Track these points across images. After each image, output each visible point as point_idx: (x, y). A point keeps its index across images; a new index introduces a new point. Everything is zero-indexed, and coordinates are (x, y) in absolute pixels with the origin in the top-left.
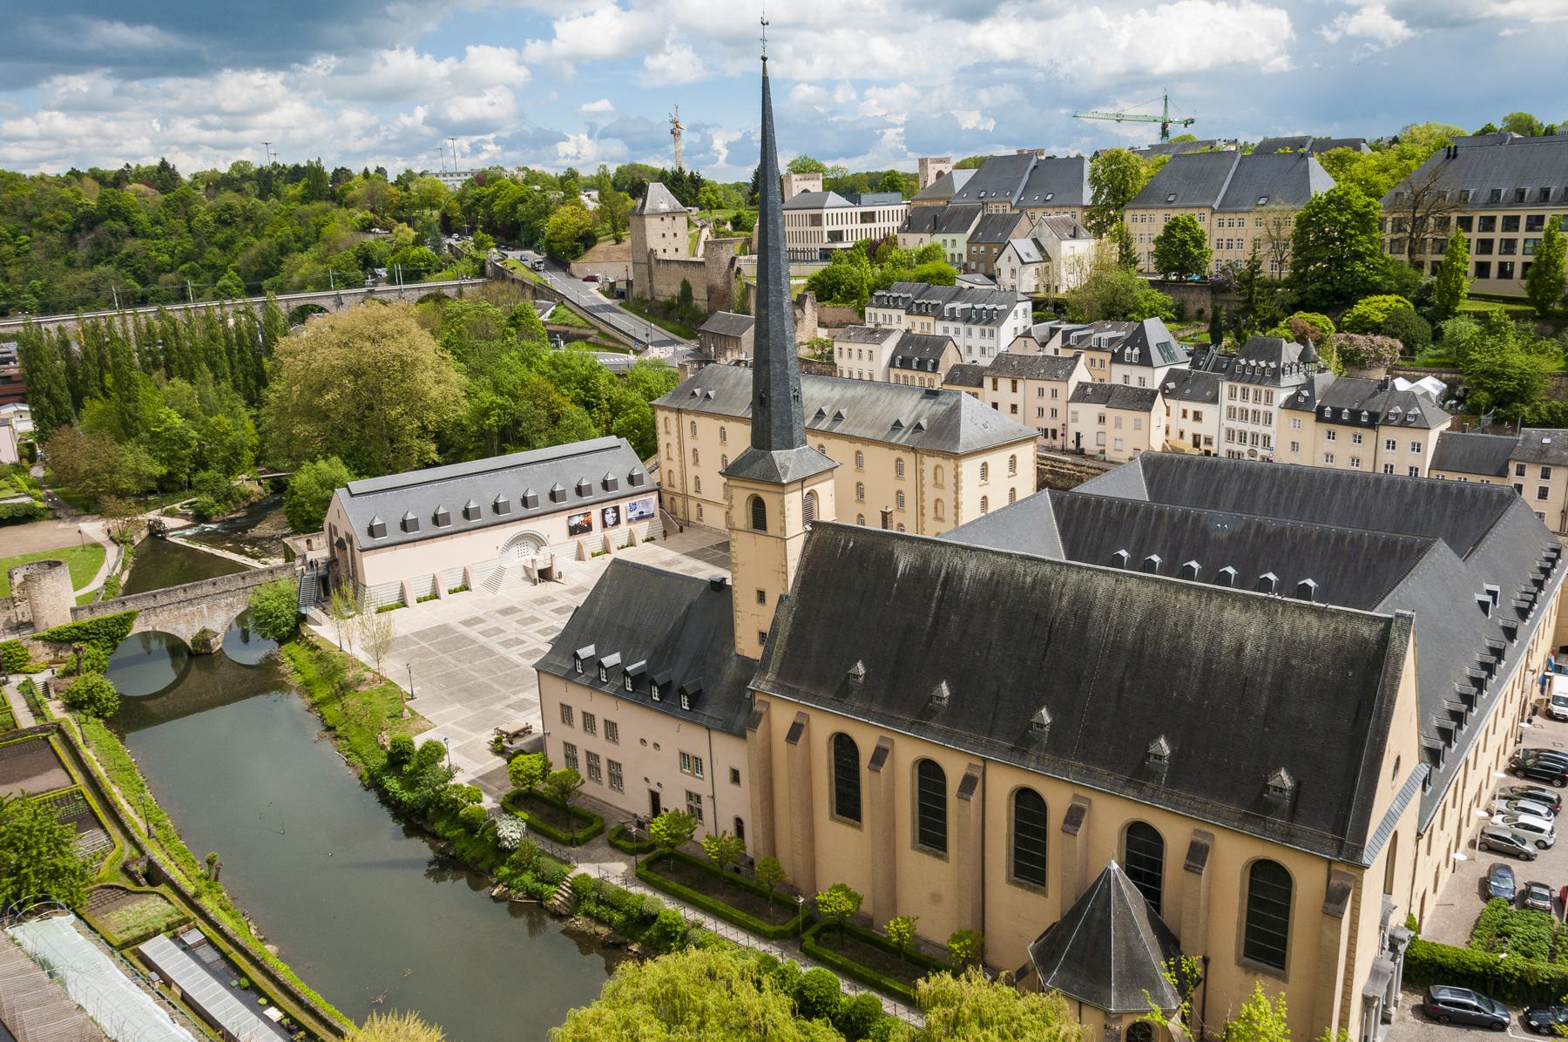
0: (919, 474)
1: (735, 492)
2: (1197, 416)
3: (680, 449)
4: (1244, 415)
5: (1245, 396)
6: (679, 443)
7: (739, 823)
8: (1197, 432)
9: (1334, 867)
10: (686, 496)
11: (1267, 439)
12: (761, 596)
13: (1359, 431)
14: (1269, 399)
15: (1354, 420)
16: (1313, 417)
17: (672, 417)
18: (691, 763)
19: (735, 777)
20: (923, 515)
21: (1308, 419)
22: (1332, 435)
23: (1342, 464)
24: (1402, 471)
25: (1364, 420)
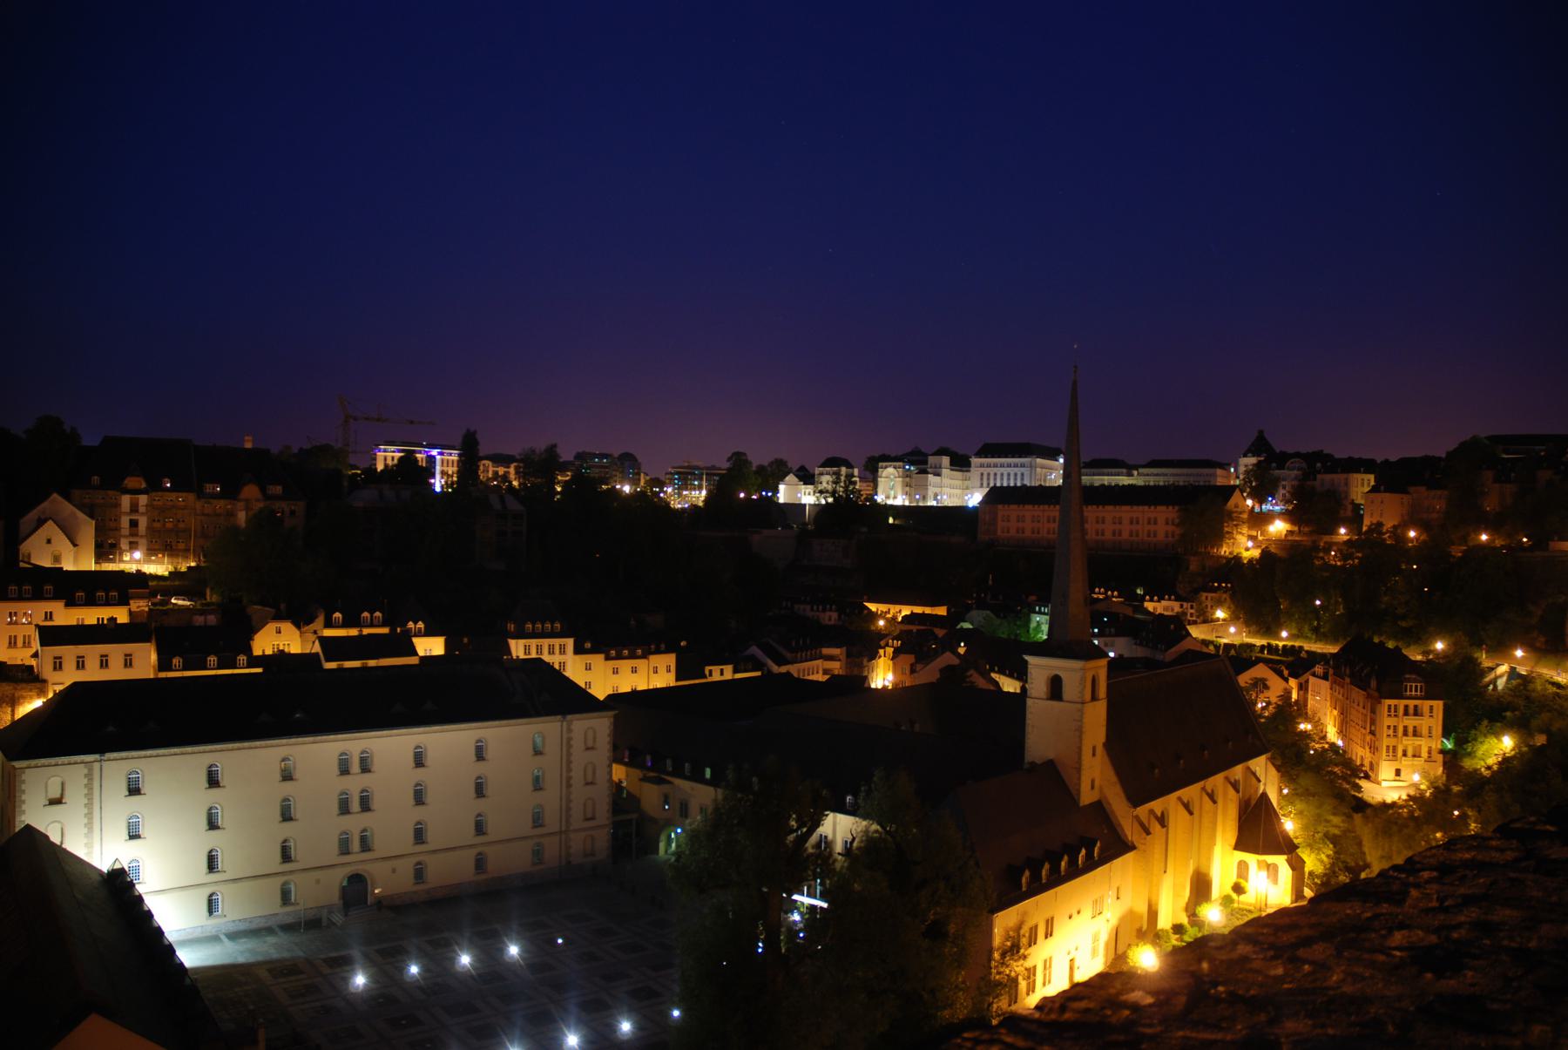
14: (563, 651)
15: (633, 656)
22: (616, 671)
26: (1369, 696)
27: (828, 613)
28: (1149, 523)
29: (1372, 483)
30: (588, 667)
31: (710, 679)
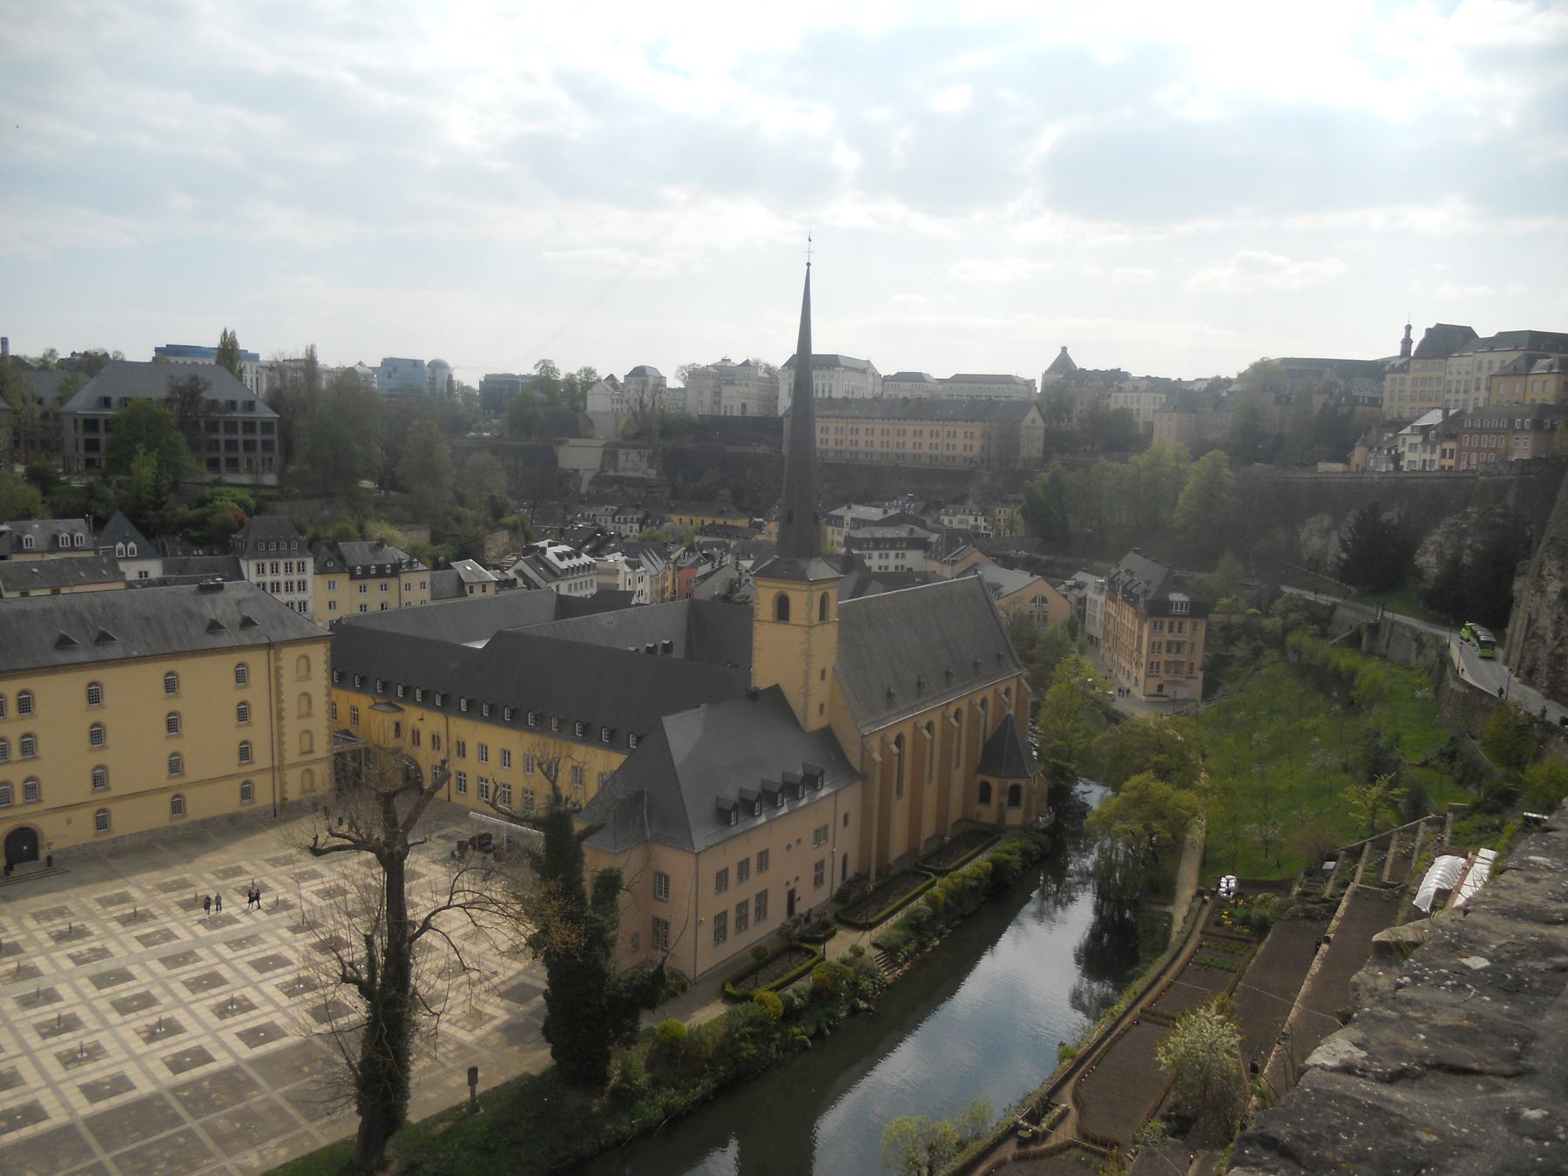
0: (275, 677)
5: (275, 570)
7: (845, 857)
13: (385, 580)
14: (302, 568)
15: (381, 572)
16: (347, 576)
20: (280, 718)
21: (342, 580)
22: (363, 589)
24: (415, 603)
25: (389, 571)
26: (1137, 614)
28: (949, 436)
29: (1164, 401)
30: (331, 585)
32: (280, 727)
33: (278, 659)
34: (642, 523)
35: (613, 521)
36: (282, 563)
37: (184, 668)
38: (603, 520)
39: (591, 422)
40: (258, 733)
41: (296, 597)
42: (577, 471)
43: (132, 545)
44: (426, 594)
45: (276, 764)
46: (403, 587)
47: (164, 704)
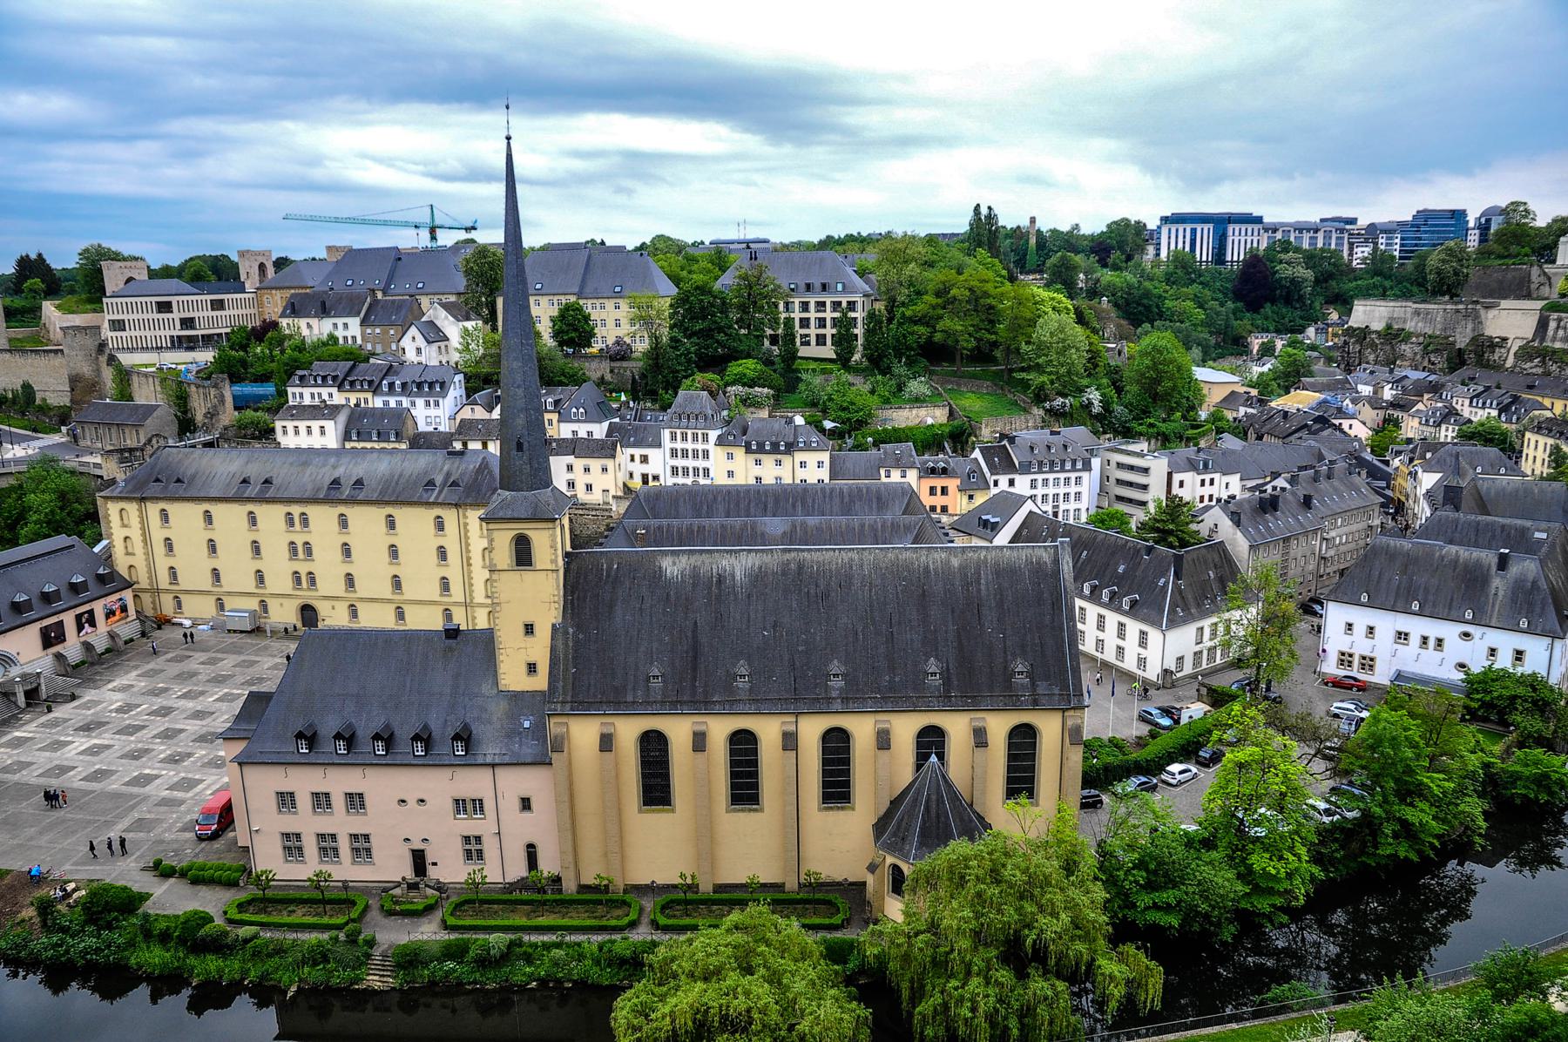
1: (496, 534)
2: (645, 459)
3: (145, 541)
4: (685, 453)
5: (684, 438)
6: (144, 534)
8: (645, 472)
9: (1066, 714)
10: (156, 591)
11: (706, 472)
12: (529, 629)
13: (779, 457)
14: (705, 438)
15: (775, 449)
16: (744, 449)
17: (132, 508)
18: (467, 806)
19: (526, 804)
20: (469, 565)
21: (739, 453)
22: (758, 462)
23: (768, 480)
24: (812, 480)
27: (1487, 410)
31: (884, 479)
32: (470, 572)
33: (465, 517)
34: (1503, 409)
35: (1471, 402)
36: (689, 432)
37: (400, 513)
38: (1460, 403)
39: (1549, 279)
40: (454, 572)
41: (700, 463)
42: (1505, 339)
43: (581, 410)
44: (824, 474)
45: (468, 601)
46: (797, 465)
47: (384, 540)
